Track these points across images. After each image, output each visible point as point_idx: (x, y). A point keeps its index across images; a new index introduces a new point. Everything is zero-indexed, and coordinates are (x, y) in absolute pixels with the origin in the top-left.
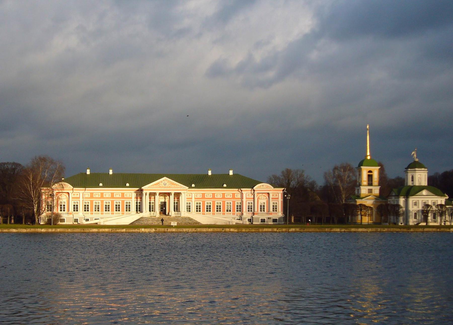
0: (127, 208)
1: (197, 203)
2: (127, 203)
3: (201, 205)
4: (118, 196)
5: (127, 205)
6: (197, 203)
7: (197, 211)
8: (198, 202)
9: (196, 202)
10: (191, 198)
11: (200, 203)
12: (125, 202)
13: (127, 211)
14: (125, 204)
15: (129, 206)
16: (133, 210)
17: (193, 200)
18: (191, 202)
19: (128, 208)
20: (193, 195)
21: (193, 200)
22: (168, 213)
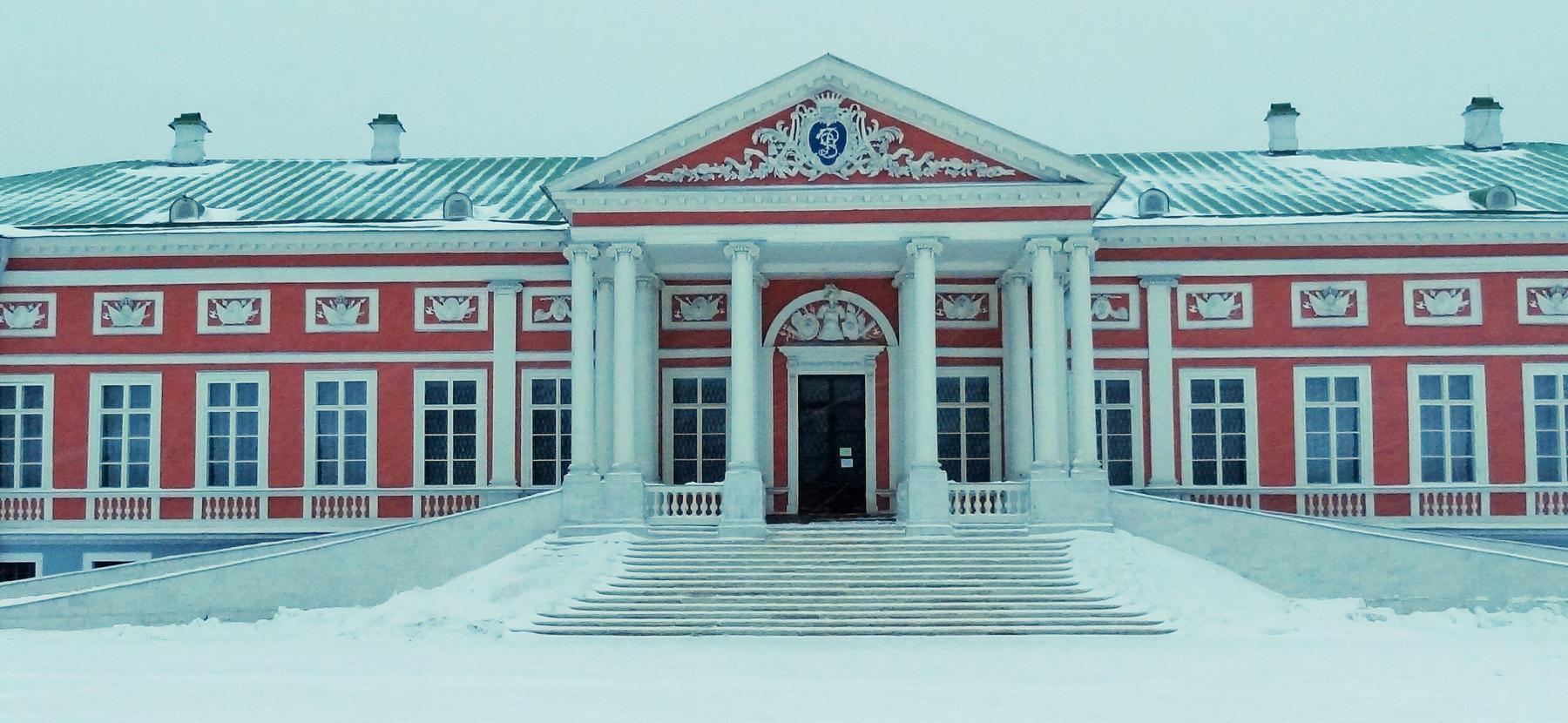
0: (434, 447)
1: (1202, 391)
2: (435, 392)
3: (1250, 405)
4: (343, 320)
5: (435, 421)
6: (1202, 391)
7: (1204, 474)
8: (1217, 375)
9: (1187, 376)
10: (1140, 338)
11: (1234, 390)
12: (421, 379)
13: (434, 474)
15: (466, 421)
17: (1161, 351)
18: (1134, 378)
19: (452, 454)
20: (1159, 299)
21: (1161, 351)
22: (884, 503)
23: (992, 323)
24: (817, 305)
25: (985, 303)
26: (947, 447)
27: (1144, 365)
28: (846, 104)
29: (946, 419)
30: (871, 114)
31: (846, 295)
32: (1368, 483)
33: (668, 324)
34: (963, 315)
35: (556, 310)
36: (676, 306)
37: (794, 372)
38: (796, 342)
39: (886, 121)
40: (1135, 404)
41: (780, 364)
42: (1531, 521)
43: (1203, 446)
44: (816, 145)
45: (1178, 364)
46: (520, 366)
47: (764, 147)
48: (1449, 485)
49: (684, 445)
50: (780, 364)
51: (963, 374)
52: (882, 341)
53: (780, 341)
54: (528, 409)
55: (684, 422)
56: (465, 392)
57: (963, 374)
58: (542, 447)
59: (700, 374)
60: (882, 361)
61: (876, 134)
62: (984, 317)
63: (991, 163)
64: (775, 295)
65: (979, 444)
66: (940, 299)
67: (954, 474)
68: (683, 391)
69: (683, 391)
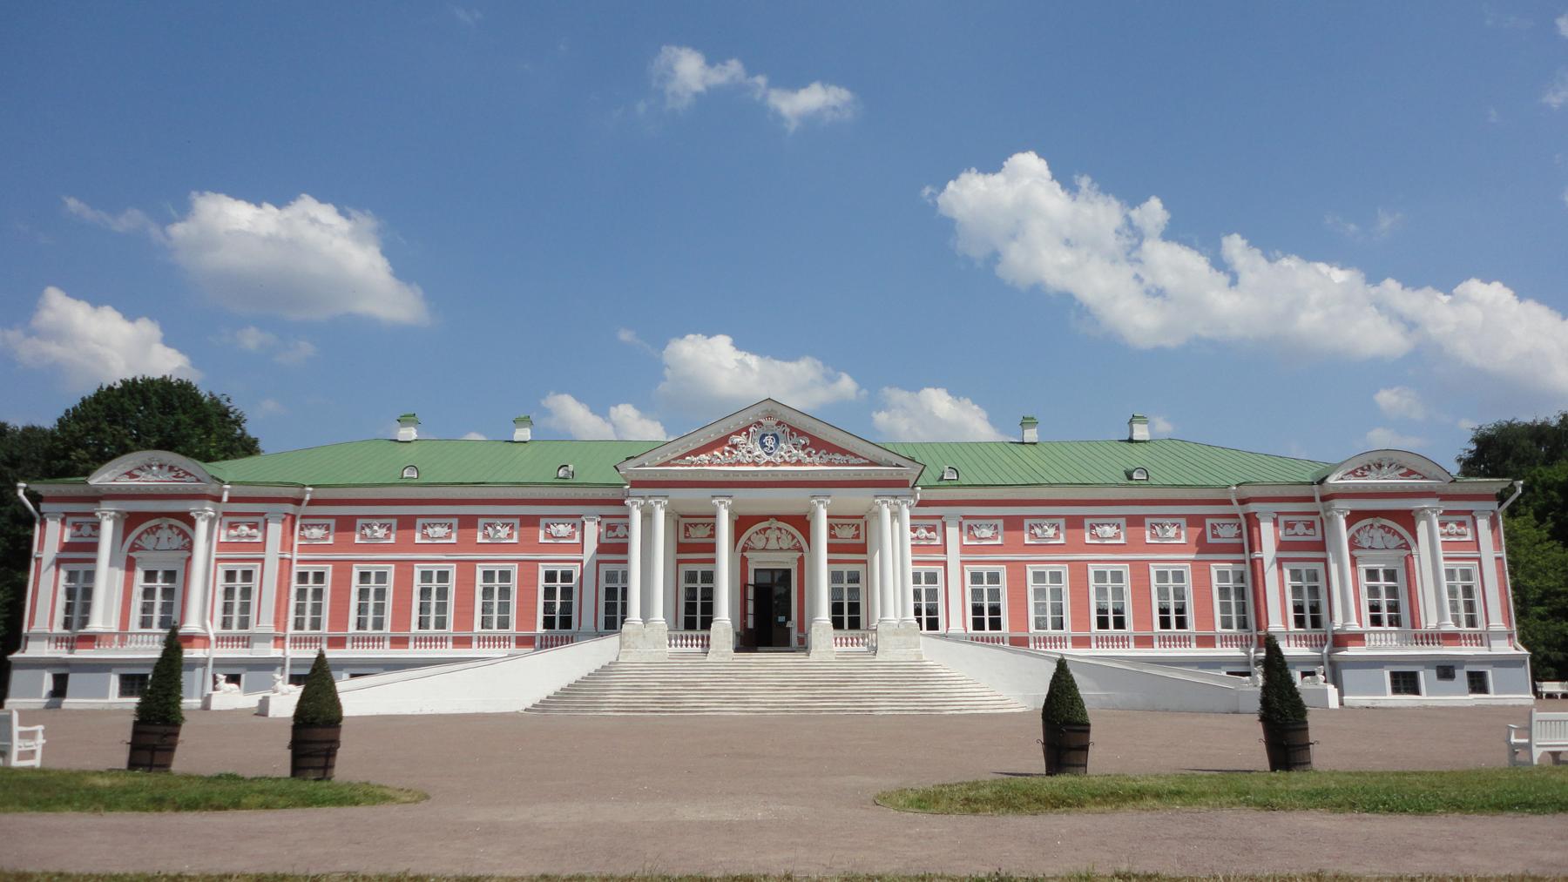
3: (1003, 586)
6: (977, 578)
7: (978, 625)
8: (985, 569)
9: (969, 570)
14: (542, 583)
16: (588, 622)
17: (954, 556)
18: (939, 570)
21: (954, 556)
23: (862, 540)
24: (765, 530)
25: (858, 528)
26: (837, 608)
27: (945, 563)
28: (779, 424)
29: (835, 593)
30: (792, 429)
31: (781, 524)
32: (1068, 630)
33: (682, 540)
34: (846, 534)
35: (620, 531)
36: (687, 530)
37: (752, 567)
38: (753, 549)
39: (801, 433)
40: (940, 586)
41: (744, 561)
42: (1157, 651)
43: (978, 610)
44: (763, 446)
45: (963, 562)
46: (598, 562)
47: (735, 446)
48: (1111, 630)
49: (690, 608)
50: (744, 561)
51: (846, 568)
52: (801, 550)
53: (744, 549)
54: (603, 586)
55: (691, 593)
56: (567, 576)
57: (846, 568)
58: (610, 608)
59: (699, 568)
60: (801, 560)
61: (795, 440)
62: (858, 536)
63: (856, 456)
64: (741, 524)
65: (854, 608)
66: (831, 527)
67: (837, 624)
68: (691, 577)
69: (691, 577)
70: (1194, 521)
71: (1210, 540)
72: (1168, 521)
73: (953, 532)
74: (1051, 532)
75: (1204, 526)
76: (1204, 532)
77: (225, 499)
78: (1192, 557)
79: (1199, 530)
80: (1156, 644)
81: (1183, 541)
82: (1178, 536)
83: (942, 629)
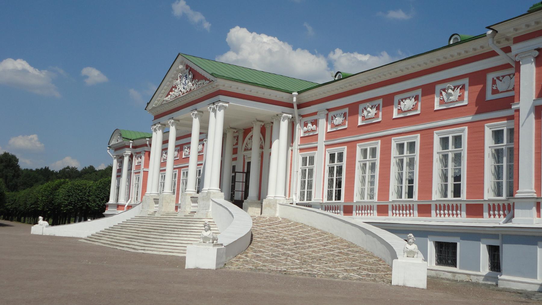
8: (336, 150)
45: (327, 146)
70: (477, 78)
71: (489, 96)
72: (451, 85)
73: (322, 122)
74: (373, 111)
75: (484, 83)
76: (483, 92)
77: (131, 147)
78: (469, 119)
79: (482, 86)
80: (433, 212)
81: (465, 102)
82: (461, 98)
83: (313, 200)
